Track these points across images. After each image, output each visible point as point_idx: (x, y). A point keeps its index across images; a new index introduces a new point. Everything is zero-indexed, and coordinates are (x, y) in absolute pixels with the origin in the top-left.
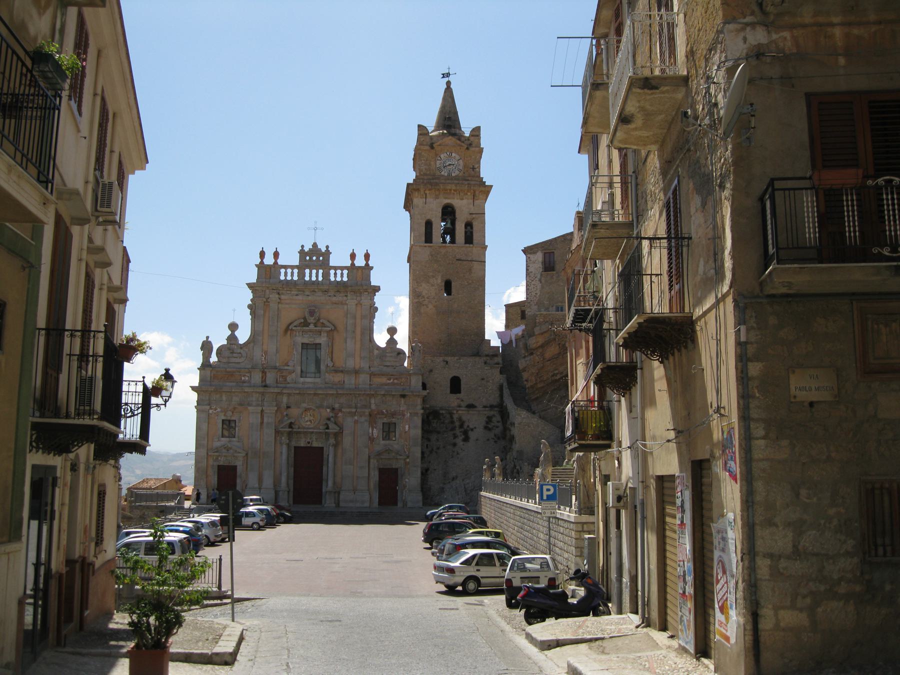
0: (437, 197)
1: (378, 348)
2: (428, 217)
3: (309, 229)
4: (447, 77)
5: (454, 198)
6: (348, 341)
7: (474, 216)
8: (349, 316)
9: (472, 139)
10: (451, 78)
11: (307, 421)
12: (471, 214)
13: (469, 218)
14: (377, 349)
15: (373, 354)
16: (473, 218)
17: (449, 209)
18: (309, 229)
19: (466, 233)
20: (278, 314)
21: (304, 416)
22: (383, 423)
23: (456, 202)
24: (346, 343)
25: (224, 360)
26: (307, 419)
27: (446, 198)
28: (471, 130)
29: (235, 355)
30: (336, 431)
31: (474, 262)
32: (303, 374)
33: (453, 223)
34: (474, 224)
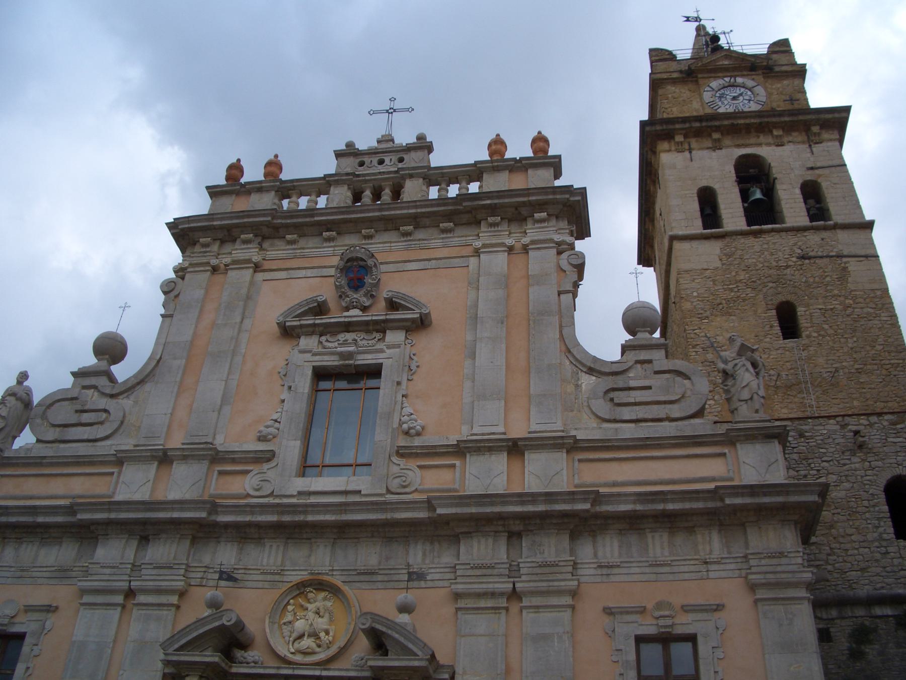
0: (717, 146)
1: (594, 368)
2: (704, 183)
3: (372, 113)
4: (696, 21)
5: (760, 145)
6: (483, 354)
7: (817, 172)
8: (481, 279)
9: (775, 56)
10: (702, 22)
11: (301, 637)
12: (812, 168)
13: (810, 175)
14: (591, 371)
15: (577, 386)
16: (819, 176)
17: (751, 170)
18: (372, 113)
19: (808, 210)
20: (248, 298)
21: (289, 617)
22: (640, 640)
23: (767, 152)
24: (473, 356)
25: (51, 434)
26: (300, 625)
27: (738, 146)
28: (768, 46)
29: (86, 418)
30: (416, 663)
31: (844, 260)
32: (305, 468)
33: (770, 191)
34: (824, 185)
